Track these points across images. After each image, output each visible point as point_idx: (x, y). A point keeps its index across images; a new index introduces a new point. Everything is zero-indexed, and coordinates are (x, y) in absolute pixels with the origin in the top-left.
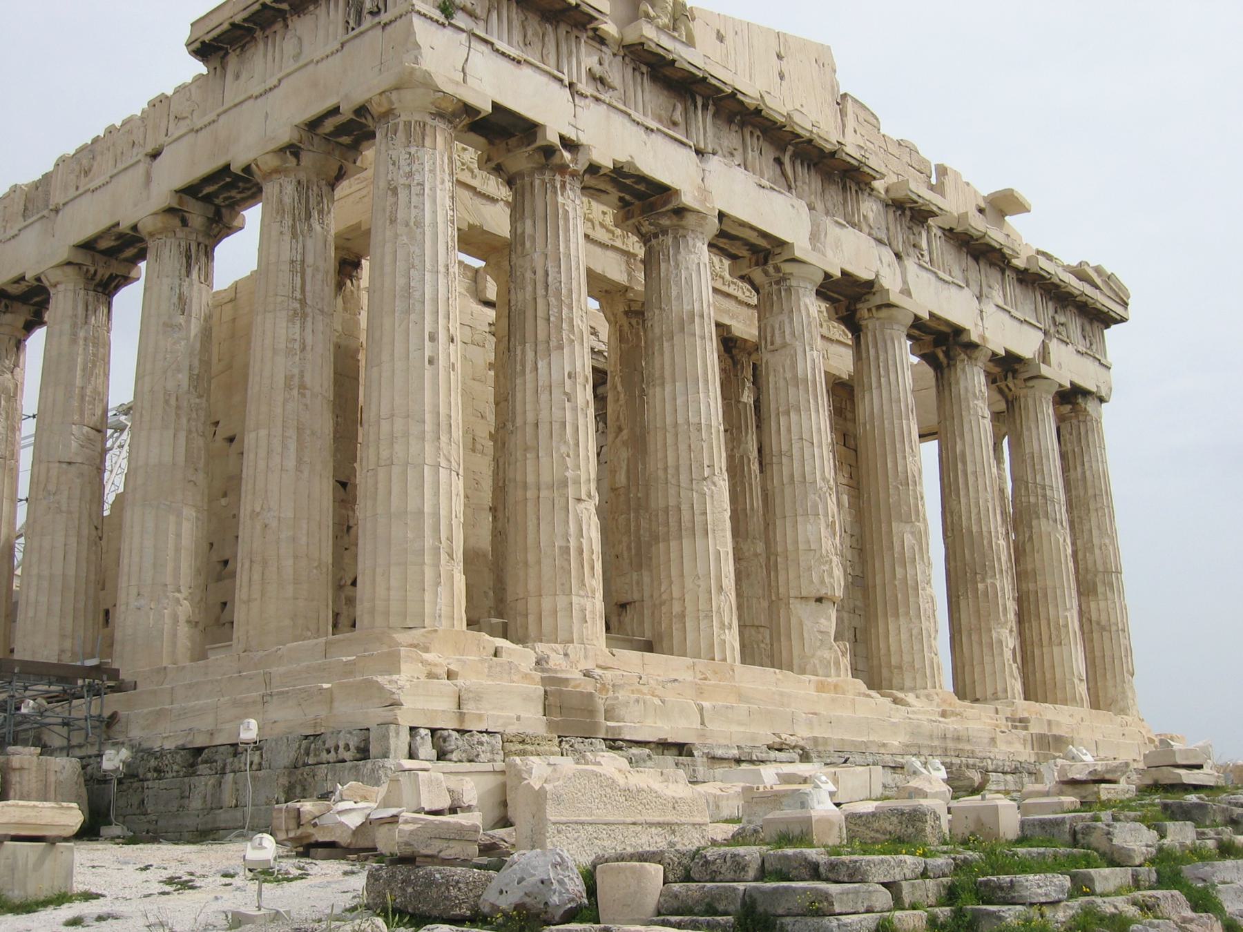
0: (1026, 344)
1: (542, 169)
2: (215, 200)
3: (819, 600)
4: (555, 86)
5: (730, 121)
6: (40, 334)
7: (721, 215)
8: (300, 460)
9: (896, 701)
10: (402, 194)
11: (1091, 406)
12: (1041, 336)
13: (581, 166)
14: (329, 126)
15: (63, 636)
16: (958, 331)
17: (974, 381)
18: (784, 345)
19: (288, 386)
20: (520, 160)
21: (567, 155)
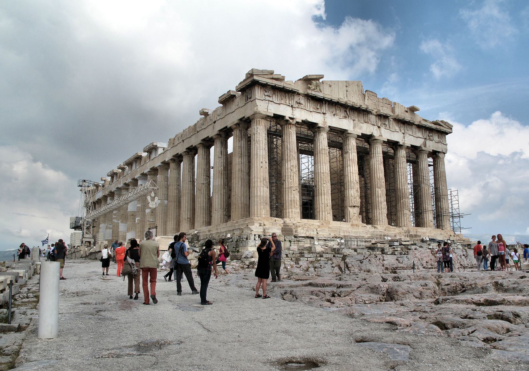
0: (418, 143)
1: (286, 124)
2: (226, 132)
3: (354, 207)
4: (288, 107)
5: (332, 105)
6: (197, 155)
7: (329, 127)
8: (241, 185)
9: (375, 227)
10: (256, 135)
11: (441, 155)
12: (423, 140)
13: (294, 122)
14: (244, 119)
15: (203, 218)
16: (397, 142)
17: (402, 154)
18: (347, 152)
19: (239, 171)
20: (282, 123)
21: (291, 121)
